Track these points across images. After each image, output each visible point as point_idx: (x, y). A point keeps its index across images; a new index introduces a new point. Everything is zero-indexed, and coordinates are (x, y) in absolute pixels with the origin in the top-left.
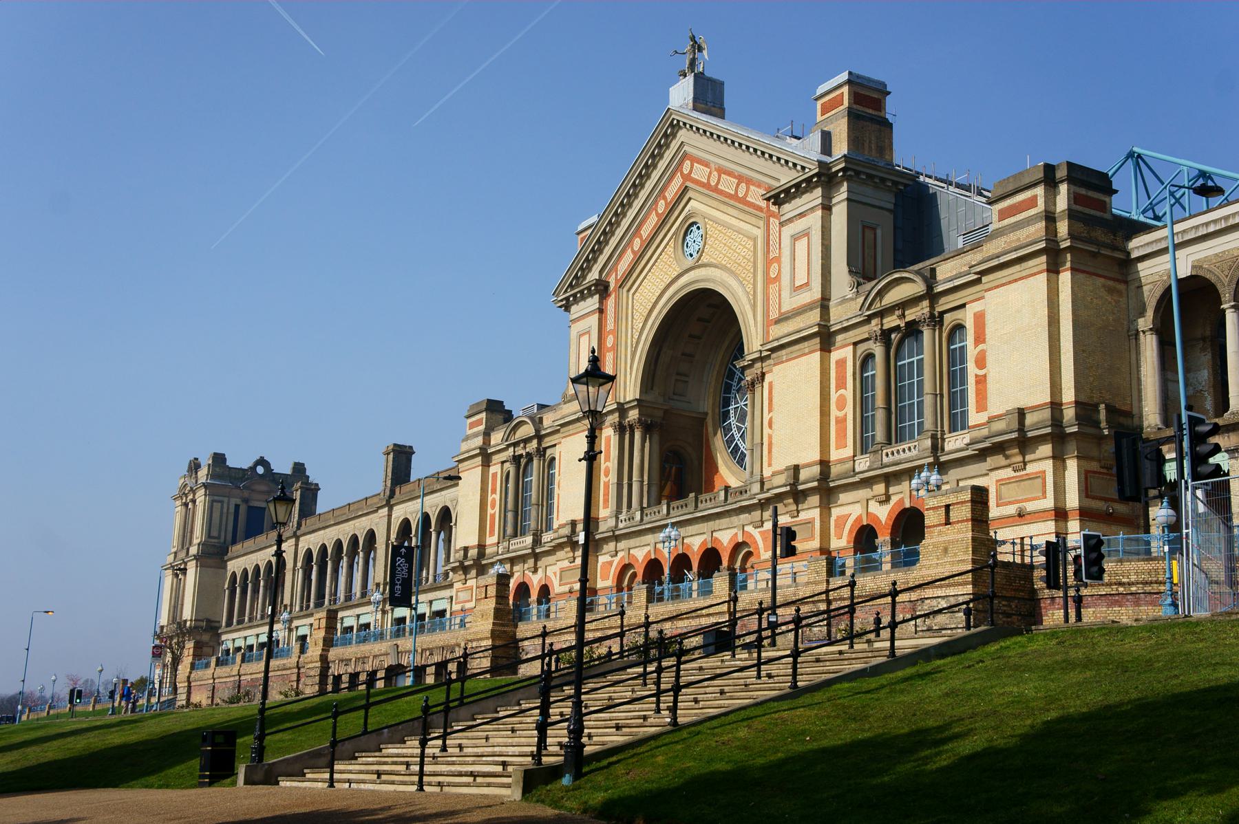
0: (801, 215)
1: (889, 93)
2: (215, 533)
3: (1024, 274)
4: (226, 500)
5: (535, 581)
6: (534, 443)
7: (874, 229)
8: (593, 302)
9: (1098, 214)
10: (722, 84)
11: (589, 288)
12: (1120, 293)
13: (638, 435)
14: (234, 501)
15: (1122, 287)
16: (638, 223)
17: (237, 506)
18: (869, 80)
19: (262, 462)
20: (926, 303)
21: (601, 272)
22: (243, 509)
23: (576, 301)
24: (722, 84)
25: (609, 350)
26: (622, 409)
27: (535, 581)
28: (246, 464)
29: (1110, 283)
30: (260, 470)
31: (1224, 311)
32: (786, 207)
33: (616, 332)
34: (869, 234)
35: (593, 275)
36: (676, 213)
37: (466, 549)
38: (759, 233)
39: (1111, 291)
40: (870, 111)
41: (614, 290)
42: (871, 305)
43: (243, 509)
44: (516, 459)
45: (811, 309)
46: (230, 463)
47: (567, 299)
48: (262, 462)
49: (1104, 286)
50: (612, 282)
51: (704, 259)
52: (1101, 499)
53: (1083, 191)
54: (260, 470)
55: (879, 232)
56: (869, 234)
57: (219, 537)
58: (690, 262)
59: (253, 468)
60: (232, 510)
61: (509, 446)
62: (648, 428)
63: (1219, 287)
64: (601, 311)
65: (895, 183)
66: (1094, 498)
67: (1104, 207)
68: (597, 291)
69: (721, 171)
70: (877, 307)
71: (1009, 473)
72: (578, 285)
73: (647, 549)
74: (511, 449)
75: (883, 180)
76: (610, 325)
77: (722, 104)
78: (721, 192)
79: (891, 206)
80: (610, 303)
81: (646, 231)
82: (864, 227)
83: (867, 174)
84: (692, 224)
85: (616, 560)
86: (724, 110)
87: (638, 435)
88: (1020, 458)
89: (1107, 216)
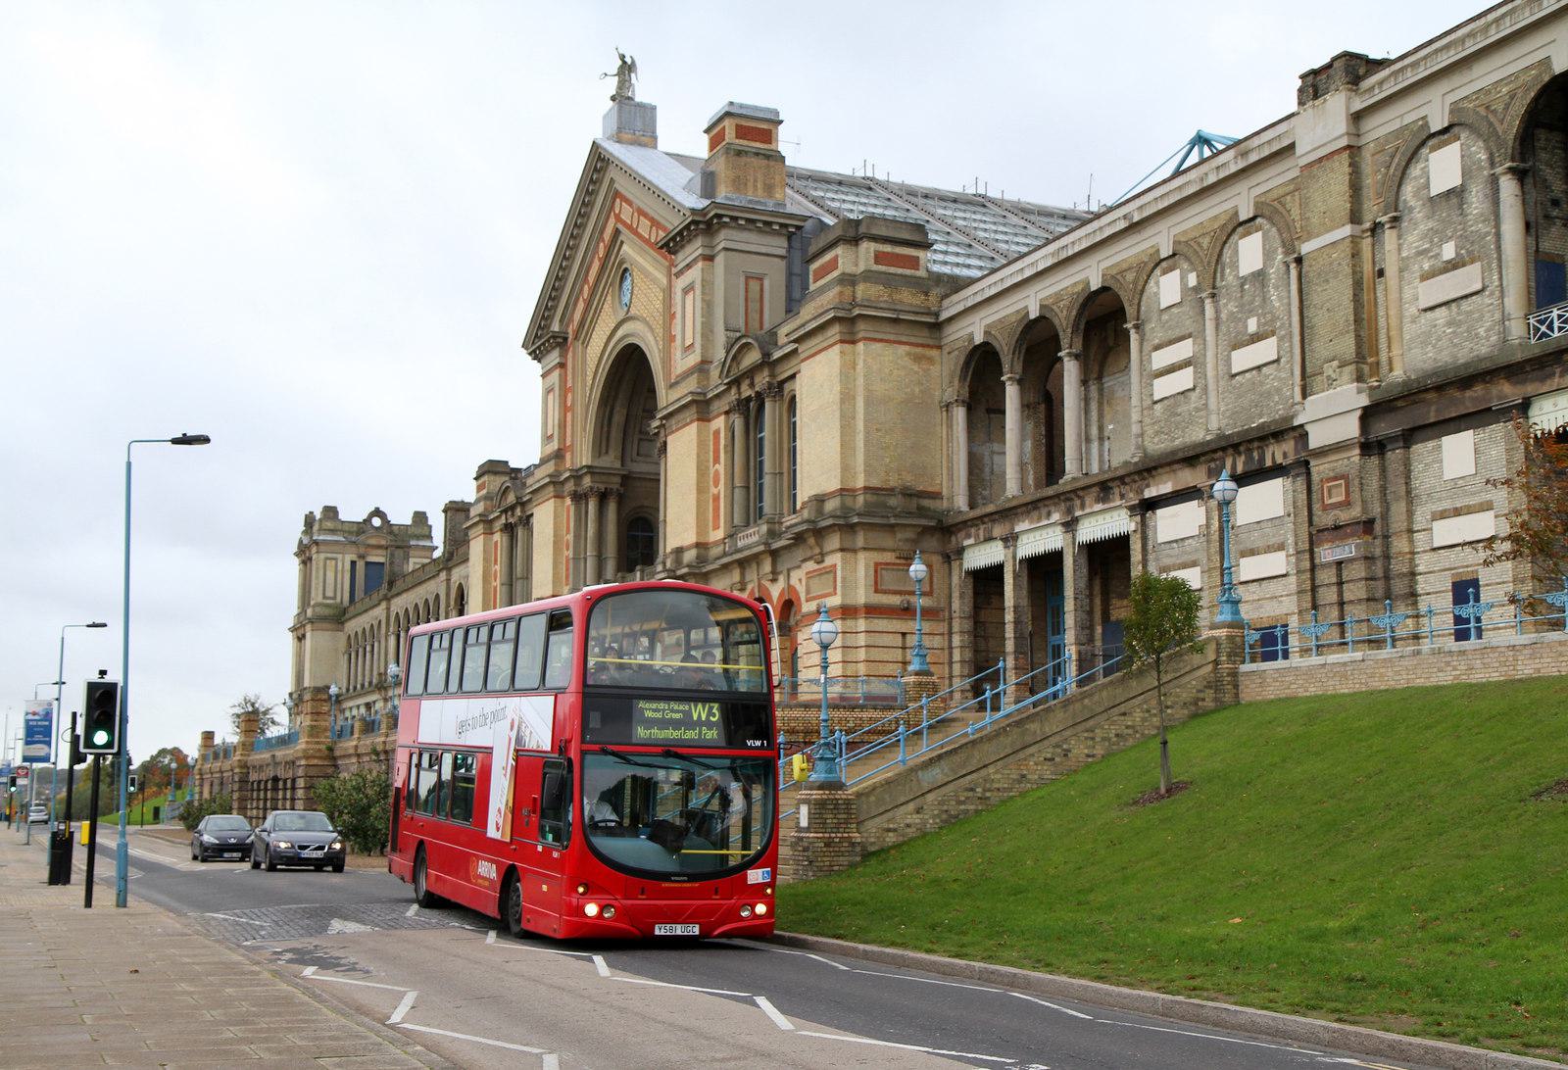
0: (689, 266)
1: (781, 122)
2: (329, 593)
3: (825, 344)
4: (340, 556)
7: (761, 279)
9: (908, 272)
10: (654, 108)
12: (930, 360)
14: (349, 558)
15: (934, 353)
16: (585, 268)
17: (353, 563)
18: (756, 108)
19: (377, 512)
20: (766, 372)
22: (360, 565)
24: (654, 108)
26: (577, 476)
29: (919, 350)
30: (377, 522)
31: (1004, 383)
32: (680, 256)
34: (754, 286)
38: (665, 281)
39: (917, 359)
40: (758, 145)
42: (728, 371)
43: (360, 565)
45: (692, 374)
46: (343, 517)
48: (377, 512)
49: (909, 354)
51: (633, 311)
52: (895, 593)
53: (888, 248)
54: (377, 522)
55: (766, 283)
56: (754, 286)
57: (334, 598)
58: (621, 315)
59: (368, 521)
60: (348, 566)
62: (603, 498)
63: (1001, 354)
64: (562, 365)
65: (783, 226)
66: (885, 592)
67: (914, 262)
68: (559, 345)
69: (641, 213)
70: (735, 373)
71: (811, 566)
75: (768, 224)
77: (654, 132)
78: (640, 236)
79: (783, 252)
81: (591, 278)
82: (747, 278)
83: (748, 220)
84: (626, 270)
86: (655, 138)
87: (592, 506)
88: (817, 550)
89: (922, 273)
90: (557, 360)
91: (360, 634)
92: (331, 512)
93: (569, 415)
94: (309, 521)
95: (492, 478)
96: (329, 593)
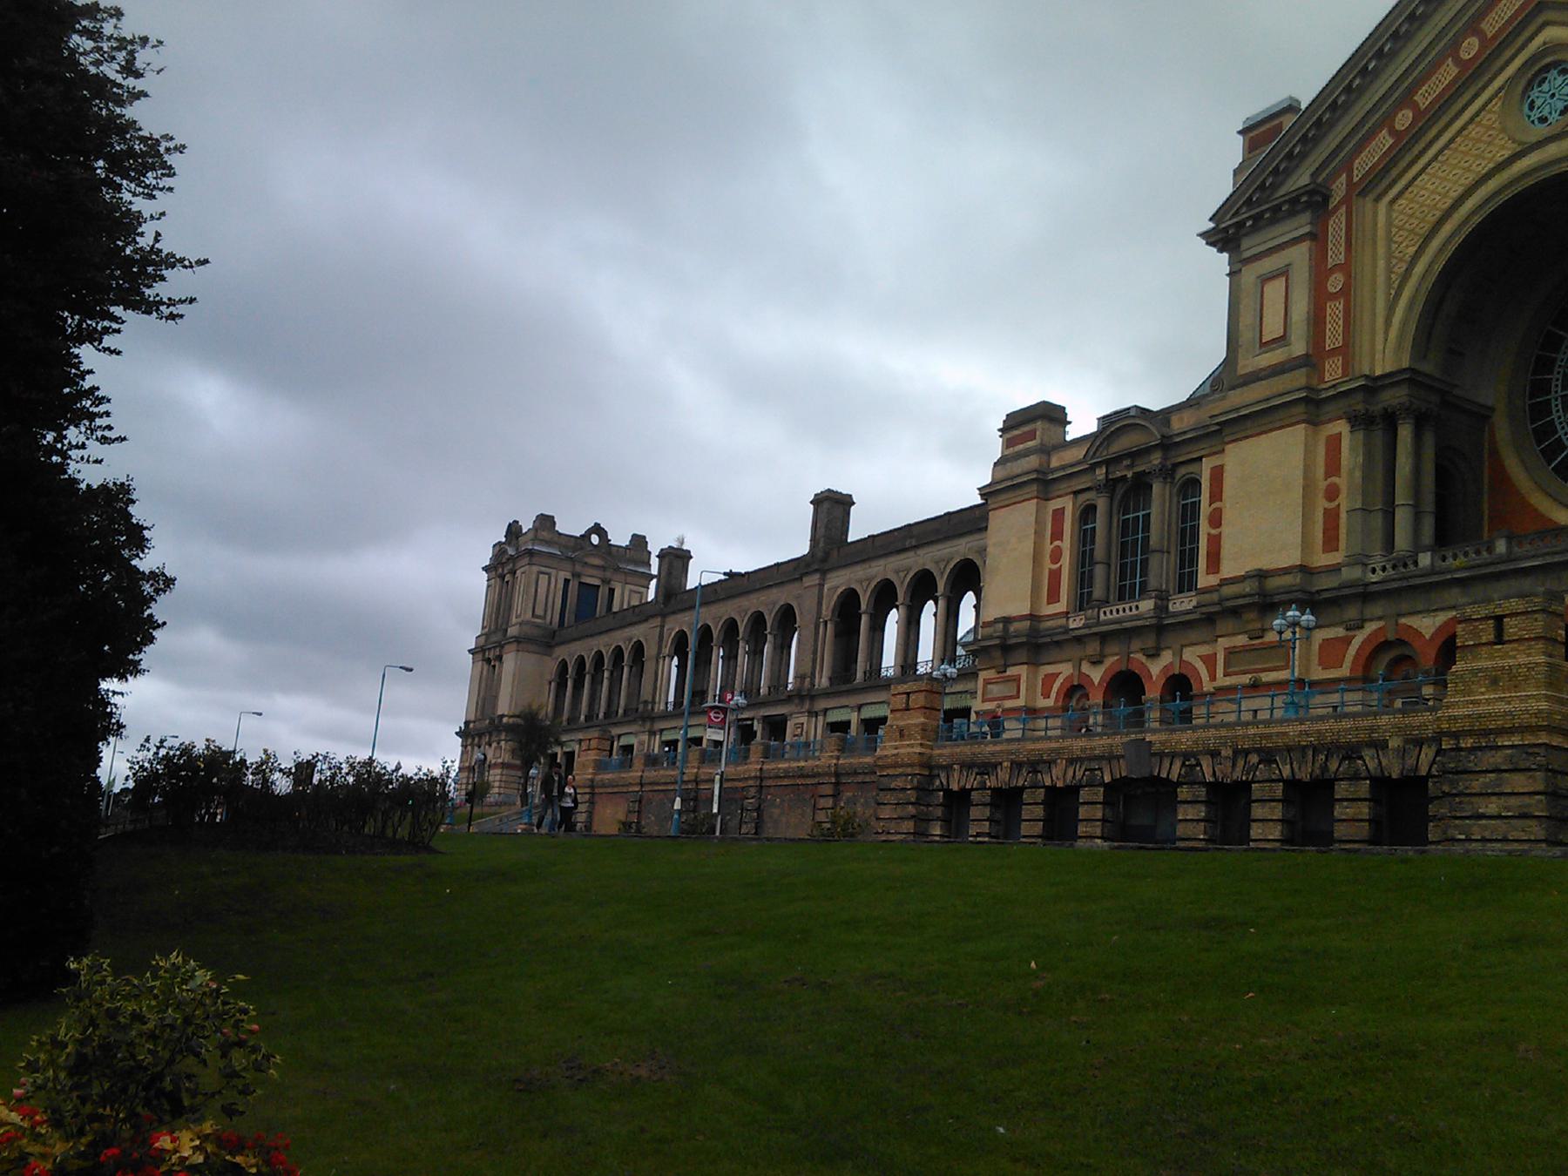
2: (539, 612)
4: (553, 572)
5: (1156, 669)
6: (1156, 459)
8: (1301, 224)
11: (1294, 201)
13: (1405, 433)
14: (563, 575)
17: (567, 581)
19: (597, 529)
21: (1314, 175)
22: (573, 586)
23: (1255, 228)
25: (1334, 297)
26: (1374, 385)
27: (1156, 669)
28: (578, 532)
30: (595, 539)
33: (1345, 268)
35: (1301, 179)
36: (1508, 54)
37: (1007, 621)
41: (1347, 200)
43: (573, 586)
44: (1110, 485)
47: (1240, 225)
48: (597, 529)
50: (1339, 188)
54: (595, 539)
57: (544, 617)
59: (586, 536)
60: (561, 585)
61: (1098, 464)
68: (1309, 205)
72: (1259, 203)
73: (1442, 618)
74: (1101, 473)
76: (1336, 255)
80: (1336, 226)
85: (1359, 638)
87: (1405, 433)
90: (1307, 229)
91: (692, 641)
92: (545, 522)
93: (1334, 310)
94: (513, 530)
95: (1047, 425)
96: (539, 612)
